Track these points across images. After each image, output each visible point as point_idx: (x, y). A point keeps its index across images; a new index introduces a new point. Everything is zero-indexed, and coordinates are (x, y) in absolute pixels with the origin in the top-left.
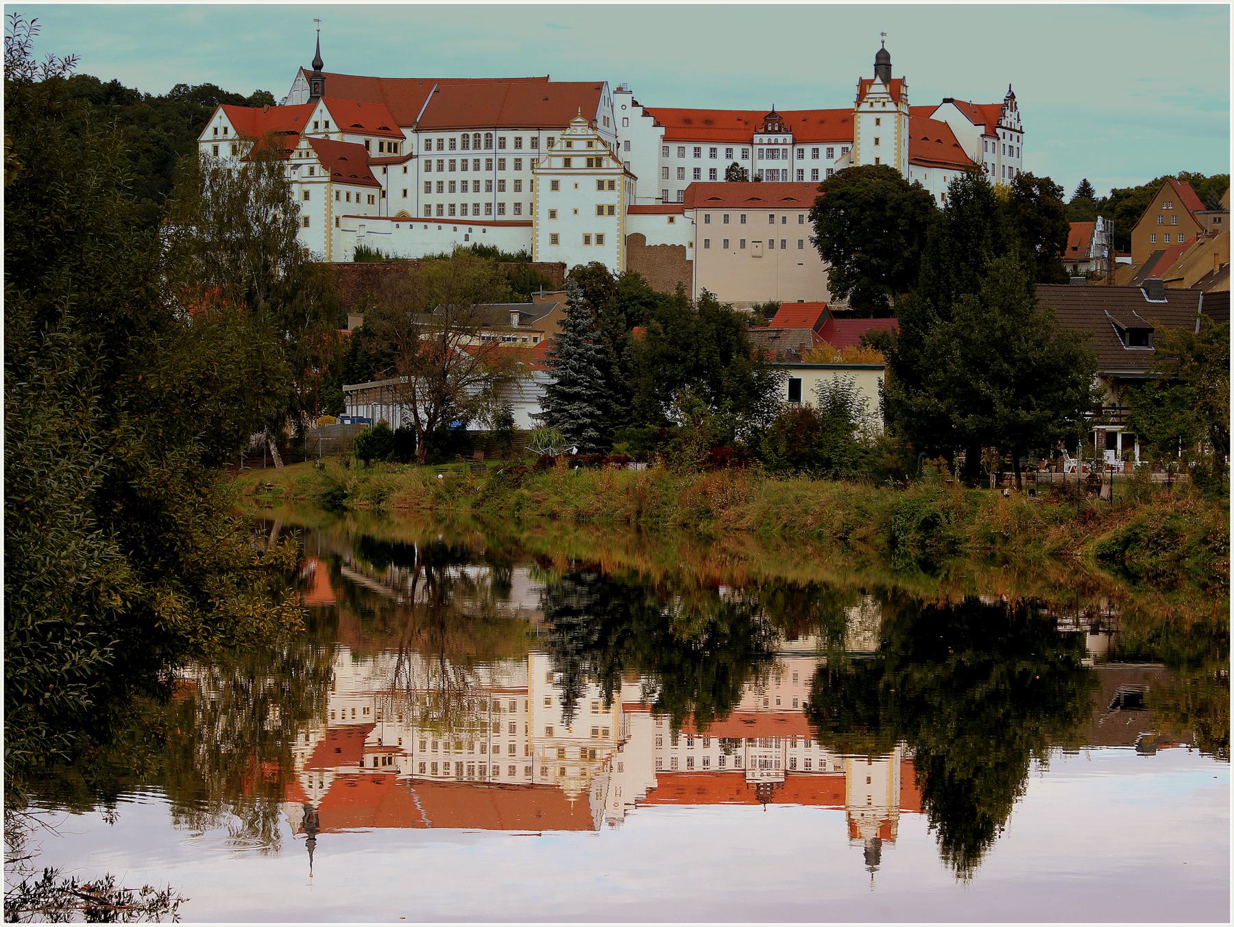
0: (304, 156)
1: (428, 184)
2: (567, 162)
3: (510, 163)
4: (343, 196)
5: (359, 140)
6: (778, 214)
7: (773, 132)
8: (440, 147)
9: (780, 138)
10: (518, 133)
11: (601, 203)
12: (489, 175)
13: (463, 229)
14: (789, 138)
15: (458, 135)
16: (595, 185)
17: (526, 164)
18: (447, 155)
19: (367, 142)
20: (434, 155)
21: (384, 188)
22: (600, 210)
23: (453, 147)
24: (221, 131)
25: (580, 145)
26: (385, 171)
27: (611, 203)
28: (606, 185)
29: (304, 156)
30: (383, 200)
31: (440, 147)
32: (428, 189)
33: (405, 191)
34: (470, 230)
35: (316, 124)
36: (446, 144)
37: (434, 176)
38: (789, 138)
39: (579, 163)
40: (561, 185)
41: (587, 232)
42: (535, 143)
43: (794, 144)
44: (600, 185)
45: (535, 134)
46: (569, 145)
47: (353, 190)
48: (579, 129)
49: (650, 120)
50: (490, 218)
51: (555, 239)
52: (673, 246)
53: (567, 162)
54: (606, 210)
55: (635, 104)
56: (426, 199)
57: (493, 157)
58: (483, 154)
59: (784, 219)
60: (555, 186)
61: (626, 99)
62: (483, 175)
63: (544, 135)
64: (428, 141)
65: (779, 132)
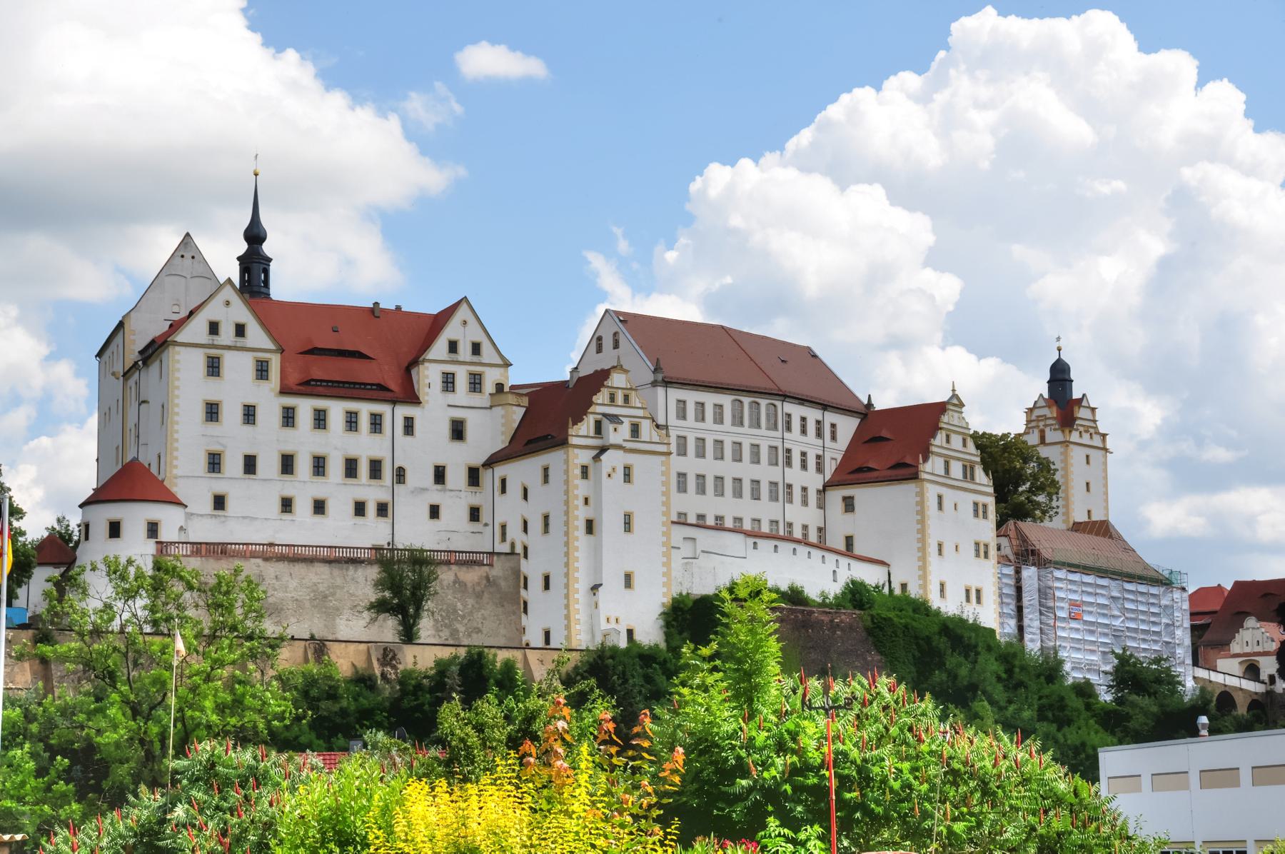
11: (978, 539)
12: (775, 474)
15: (726, 400)
20: (690, 428)
23: (719, 419)
31: (701, 417)
32: (682, 488)
37: (690, 464)
39: (957, 470)
57: (778, 443)
58: (766, 438)
62: (766, 473)
63: (830, 418)
64: (682, 403)
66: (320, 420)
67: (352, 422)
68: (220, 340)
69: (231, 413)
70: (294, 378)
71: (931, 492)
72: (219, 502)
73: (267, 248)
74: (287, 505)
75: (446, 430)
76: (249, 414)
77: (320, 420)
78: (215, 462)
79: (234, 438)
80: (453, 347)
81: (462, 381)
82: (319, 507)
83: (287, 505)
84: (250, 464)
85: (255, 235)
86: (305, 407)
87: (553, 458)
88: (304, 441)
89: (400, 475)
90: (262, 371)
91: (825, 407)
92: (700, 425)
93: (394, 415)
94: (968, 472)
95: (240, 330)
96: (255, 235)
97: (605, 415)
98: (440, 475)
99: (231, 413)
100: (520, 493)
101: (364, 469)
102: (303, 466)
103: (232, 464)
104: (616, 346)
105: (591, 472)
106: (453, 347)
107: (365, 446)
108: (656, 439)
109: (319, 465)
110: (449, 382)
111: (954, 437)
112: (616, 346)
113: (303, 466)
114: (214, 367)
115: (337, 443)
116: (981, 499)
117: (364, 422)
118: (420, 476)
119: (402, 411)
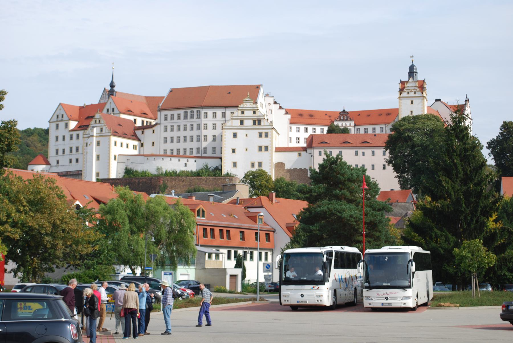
0: (98, 122)
1: (166, 138)
2: (242, 123)
3: (210, 126)
4: (119, 144)
5: (131, 118)
6: (360, 151)
7: (343, 120)
8: (172, 118)
9: (348, 123)
10: (214, 110)
11: (260, 145)
13: (183, 161)
14: (352, 123)
15: (182, 112)
16: (258, 135)
17: (219, 126)
18: (176, 122)
19: (135, 120)
20: (169, 123)
21: (142, 142)
22: (260, 149)
23: (179, 118)
24: (60, 117)
25: (249, 113)
26: (143, 133)
27: (266, 145)
28: (263, 135)
29: (98, 122)
30: (142, 148)
31: (172, 118)
32: (166, 142)
33: (153, 143)
34: (188, 161)
35: (108, 110)
37: (169, 134)
38: (352, 123)
39: (248, 123)
40: (238, 135)
41: (253, 161)
42: (224, 115)
43: (355, 126)
44: (260, 135)
45: (223, 110)
46: (243, 113)
47: (125, 141)
48: (248, 105)
49: (283, 111)
50: (200, 155)
51: (235, 165)
52: (301, 169)
53: (242, 123)
54: (263, 149)
55: (275, 103)
56: (164, 146)
58: (195, 122)
59: (363, 153)
60: (235, 135)
61: (271, 100)
63: (228, 112)
65: (347, 120)
74: (71, 161)
82: (77, 161)
83: (71, 161)
84: (64, 150)
91: (226, 107)
95: (63, 116)
105: (85, 145)
106: (108, 110)
108: (107, 132)
111: (245, 112)
116: (264, 131)
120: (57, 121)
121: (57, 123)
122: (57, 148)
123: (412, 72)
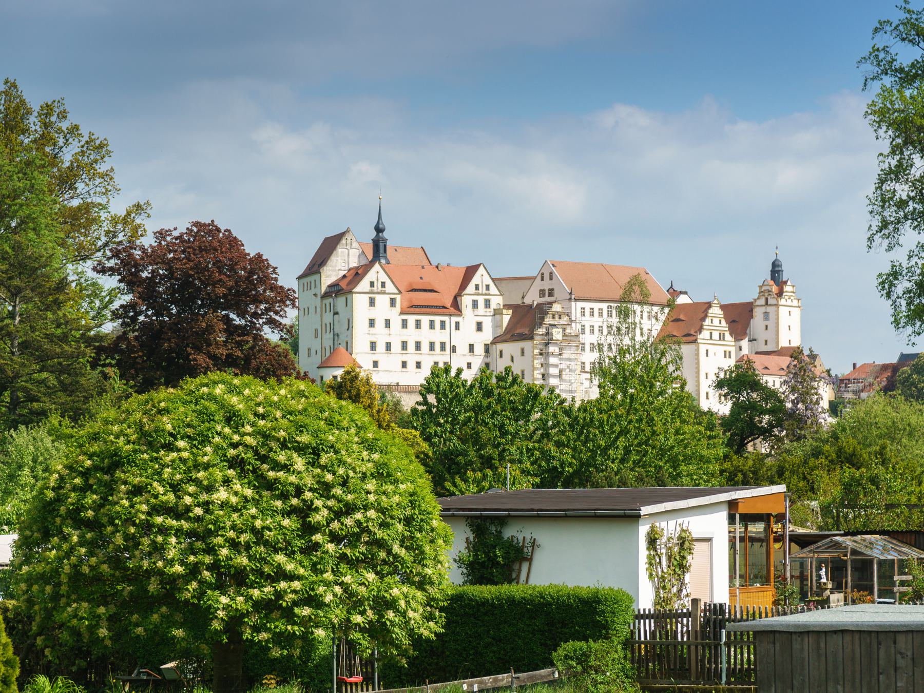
8: (592, 314)
15: (604, 306)
31: (592, 314)
36: (587, 312)
39: (716, 335)
66: (418, 325)
67: (432, 325)
68: (375, 289)
69: (380, 323)
70: (406, 304)
71: (702, 349)
72: (375, 364)
73: (385, 234)
74: (404, 364)
75: (475, 327)
76: (388, 324)
77: (418, 325)
78: (373, 346)
79: (381, 335)
80: (477, 287)
81: (481, 304)
83: (404, 364)
84: (388, 346)
85: (379, 230)
86: (412, 319)
87: (527, 345)
88: (411, 335)
89: (454, 349)
90: (393, 303)
92: (592, 319)
93: (451, 321)
94: (722, 337)
96: (379, 230)
97: (551, 325)
98: (471, 347)
99: (380, 323)
100: (510, 358)
101: (437, 347)
102: (411, 346)
103: (381, 347)
104: (551, 278)
107: (438, 336)
109: (418, 346)
110: (475, 304)
111: (714, 320)
112: (551, 278)
113: (411, 346)
114: (372, 302)
115: (426, 335)
116: (728, 349)
117: (438, 325)
118: (463, 349)
119: (454, 319)
120: (371, 292)
121: (372, 296)
122: (374, 340)
123: (776, 271)
